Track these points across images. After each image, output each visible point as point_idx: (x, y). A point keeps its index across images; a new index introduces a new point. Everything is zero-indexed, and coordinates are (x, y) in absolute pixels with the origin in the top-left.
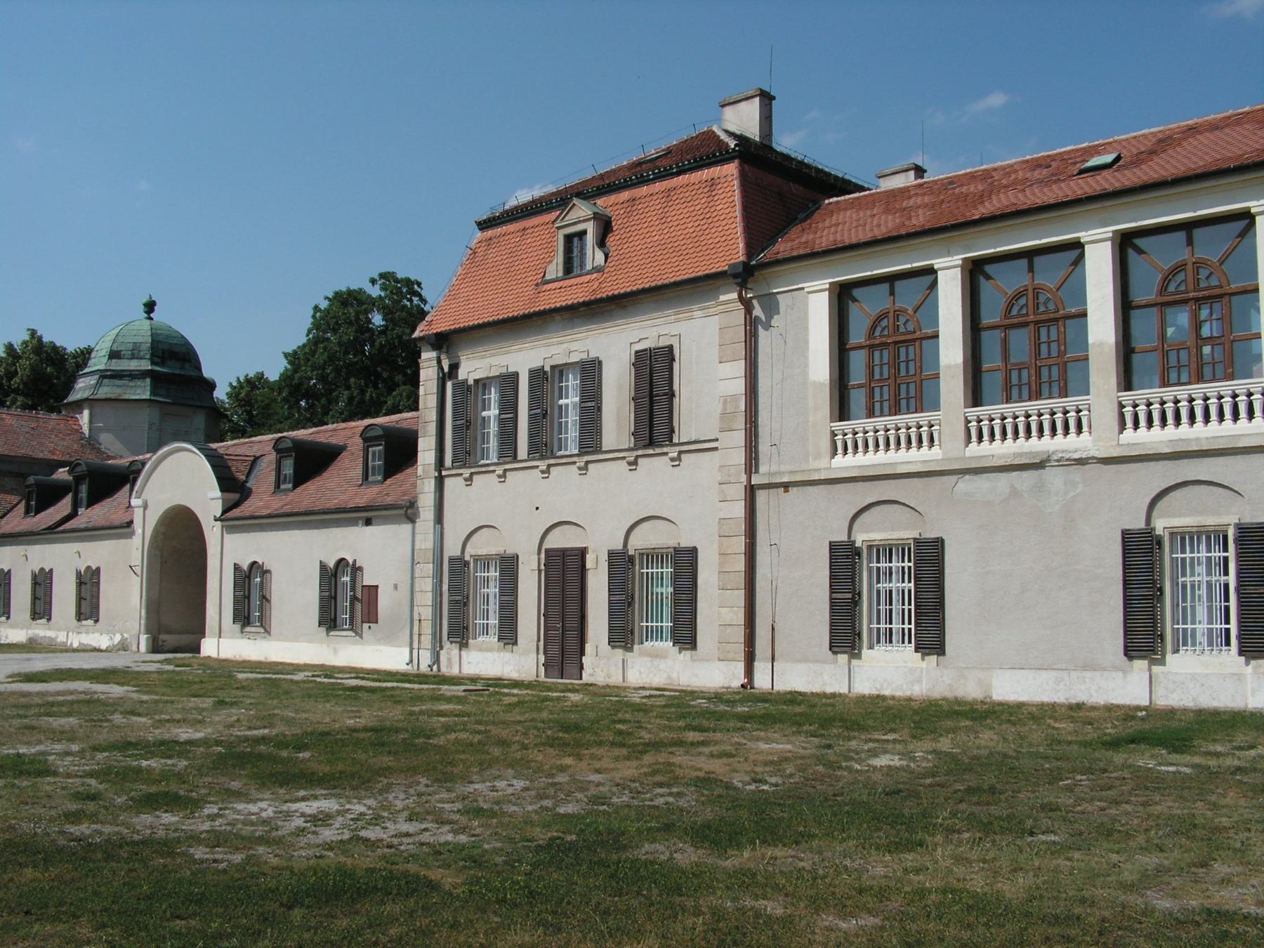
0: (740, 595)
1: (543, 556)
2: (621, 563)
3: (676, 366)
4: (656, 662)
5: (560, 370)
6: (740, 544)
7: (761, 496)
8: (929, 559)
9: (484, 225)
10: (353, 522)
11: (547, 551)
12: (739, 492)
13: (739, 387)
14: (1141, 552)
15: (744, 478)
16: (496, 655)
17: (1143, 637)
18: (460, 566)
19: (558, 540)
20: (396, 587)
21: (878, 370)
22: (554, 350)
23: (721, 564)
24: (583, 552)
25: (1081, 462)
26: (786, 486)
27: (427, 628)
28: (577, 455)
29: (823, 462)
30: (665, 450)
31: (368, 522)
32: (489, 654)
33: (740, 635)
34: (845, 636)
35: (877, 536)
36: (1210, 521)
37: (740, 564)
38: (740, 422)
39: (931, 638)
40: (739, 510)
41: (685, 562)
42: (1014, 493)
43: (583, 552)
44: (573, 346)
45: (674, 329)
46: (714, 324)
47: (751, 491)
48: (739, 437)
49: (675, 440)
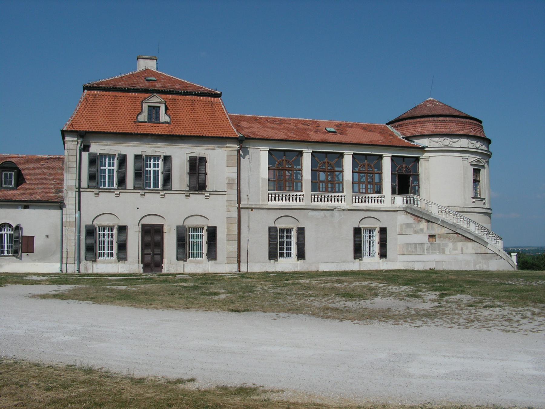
0: (236, 243)
1: (140, 226)
2: (182, 231)
3: (207, 165)
4: (198, 265)
5: (149, 157)
6: (236, 226)
7: (242, 211)
8: (301, 232)
9: (85, 88)
10: (16, 207)
11: (142, 224)
12: (235, 209)
13: (235, 175)
14: (358, 232)
15: (237, 205)
16: (114, 265)
17: (358, 254)
18: (91, 230)
19: (149, 221)
20: (47, 237)
21: (283, 175)
22: (145, 149)
23: (228, 232)
24: (161, 226)
25: (343, 210)
26: (252, 209)
27: (72, 255)
28: (161, 190)
29: (266, 203)
30: (203, 193)
31: (26, 207)
32: (110, 265)
33: (236, 255)
34: (273, 255)
35: (283, 225)
36: (373, 226)
37: (236, 232)
38: (236, 187)
39: (301, 255)
40: (235, 215)
41: (212, 231)
42: (325, 216)
43: (161, 226)
44: (157, 149)
45: (206, 152)
46: (225, 153)
47: (239, 209)
48: (235, 192)
49: (207, 190)
